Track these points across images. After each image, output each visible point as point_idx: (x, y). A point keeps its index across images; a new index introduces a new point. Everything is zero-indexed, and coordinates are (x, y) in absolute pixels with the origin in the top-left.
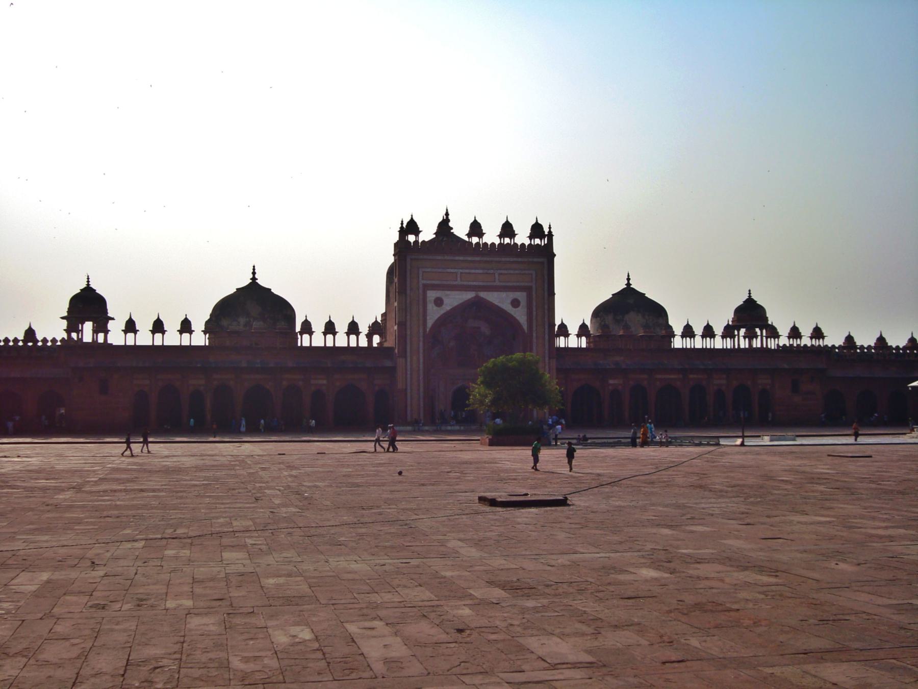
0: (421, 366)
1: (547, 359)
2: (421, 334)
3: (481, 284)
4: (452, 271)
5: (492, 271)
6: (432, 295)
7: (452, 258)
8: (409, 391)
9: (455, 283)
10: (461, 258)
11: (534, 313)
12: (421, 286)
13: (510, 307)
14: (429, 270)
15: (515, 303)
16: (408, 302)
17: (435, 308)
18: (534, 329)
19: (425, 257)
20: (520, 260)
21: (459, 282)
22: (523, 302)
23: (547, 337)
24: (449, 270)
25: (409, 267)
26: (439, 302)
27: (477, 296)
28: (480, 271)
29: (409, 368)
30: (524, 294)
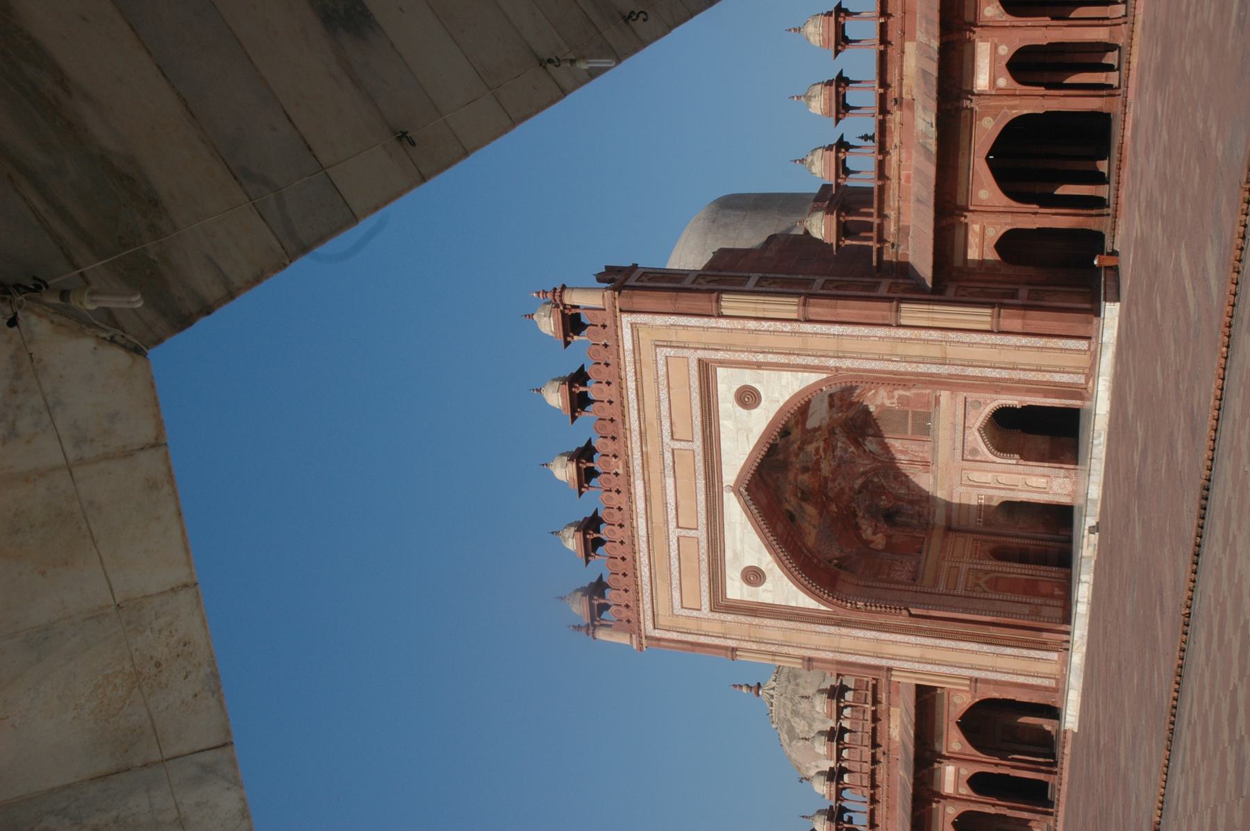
0: (912, 639)
1: (901, 333)
2: (833, 629)
3: (701, 483)
4: (674, 546)
5: (668, 456)
6: (736, 590)
7: (642, 545)
8: (976, 674)
9: (704, 544)
10: (641, 523)
11: (771, 358)
12: (717, 616)
13: (755, 412)
14: (676, 595)
15: (748, 398)
16: (754, 646)
17: (768, 585)
18: (816, 362)
19: (646, 598)
20: (631, 385)
21: (702, 534)
22: (748, 377)
23: (836, 329)
24: (674, 553)
25: (674, 636)
26: (754, 576)
27: (735, 490)
28: (670, 481)
29: (916, 666)
30: (721, 372)
